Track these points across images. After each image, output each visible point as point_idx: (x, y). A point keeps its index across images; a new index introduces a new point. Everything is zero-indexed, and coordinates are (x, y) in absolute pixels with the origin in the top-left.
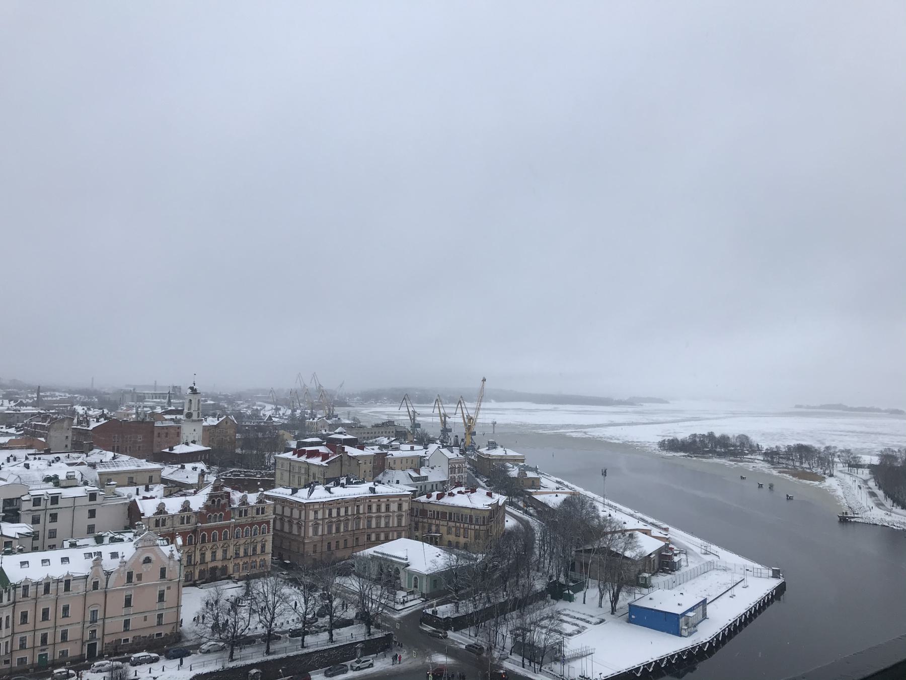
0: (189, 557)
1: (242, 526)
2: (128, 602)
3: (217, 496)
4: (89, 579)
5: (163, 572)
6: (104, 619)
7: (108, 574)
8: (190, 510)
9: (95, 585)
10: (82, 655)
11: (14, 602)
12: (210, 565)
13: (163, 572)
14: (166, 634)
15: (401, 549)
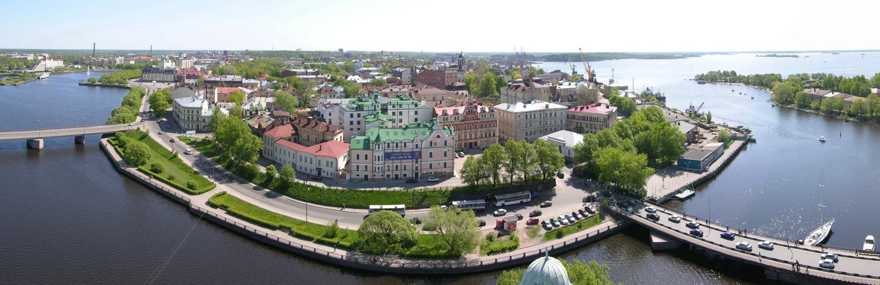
0: (459, 137)
2: (431, 156)
5: (446, 142)
13: (446, 142)
15: (561, 135)
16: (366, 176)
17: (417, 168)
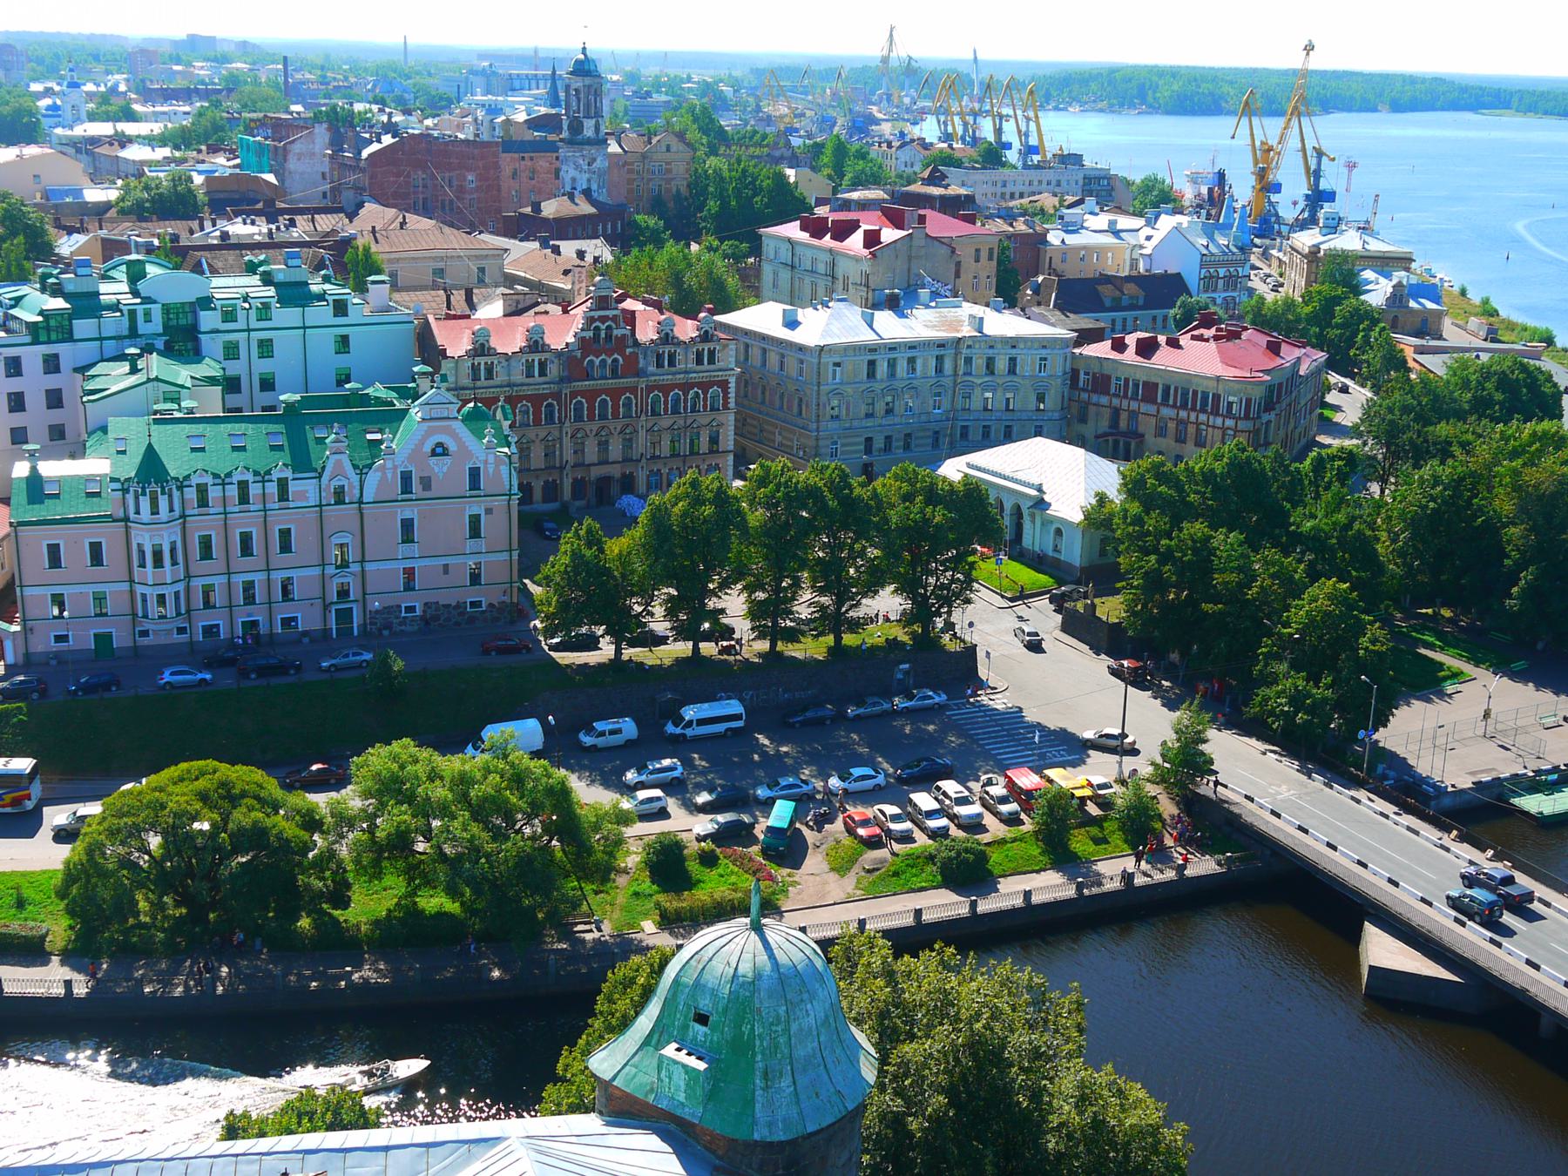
1: (666, 389)
2: (408, 537)
3: (603, 319)
5: (475, 474)
6: (363, 561)
8: (544, 348)
10: (326, 632)
11: (183, 516)
12: (596, 472)
13: (475, 474)
14: (491, 605)
16: (103, 640)
17: (343, 593)
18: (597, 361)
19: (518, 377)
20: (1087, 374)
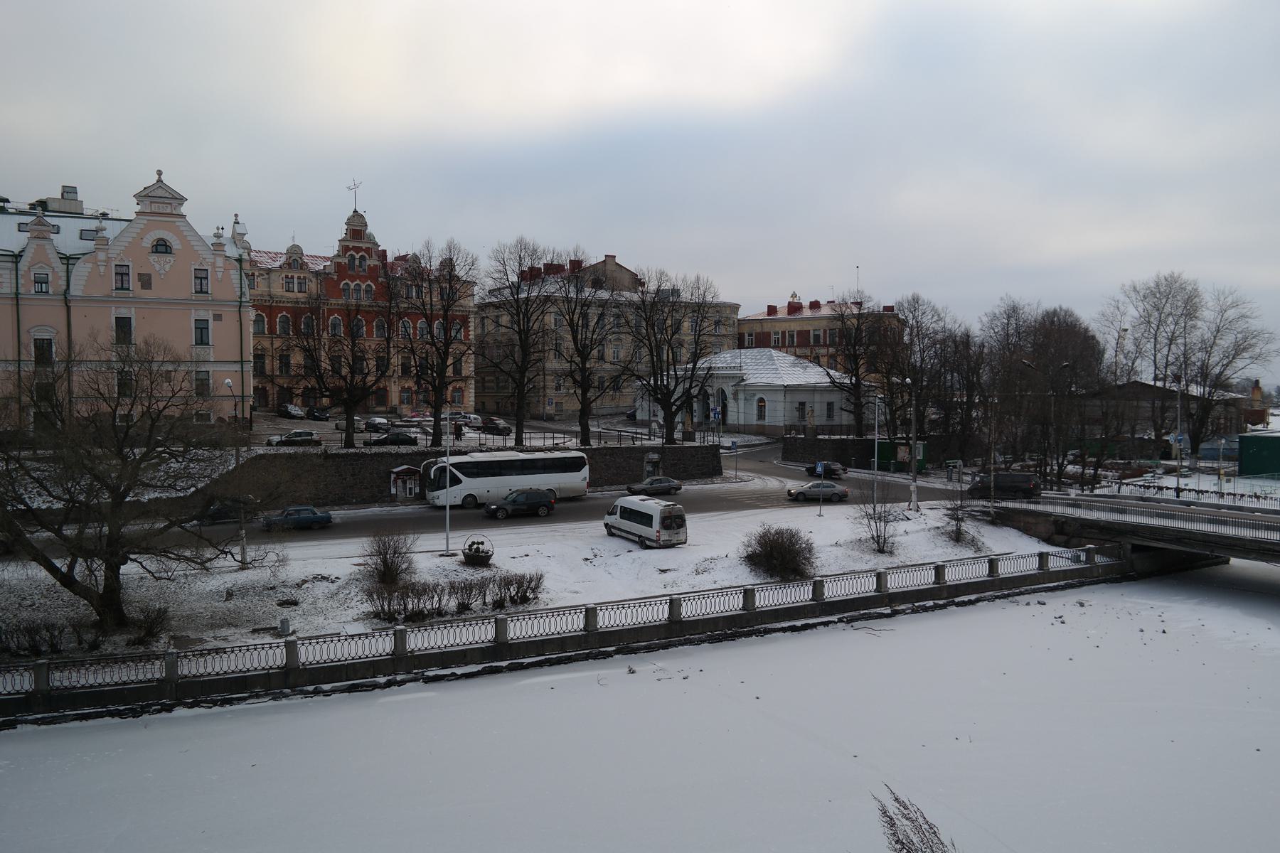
3: (358, 249)
4: (23, 265)
5: (201, 276)
7: (68, 260)
8: (303, 266)
9: (41, 281)
13: (201, 276)
18: (352, 285)
19: (278, 289)
20: (750, 335)
